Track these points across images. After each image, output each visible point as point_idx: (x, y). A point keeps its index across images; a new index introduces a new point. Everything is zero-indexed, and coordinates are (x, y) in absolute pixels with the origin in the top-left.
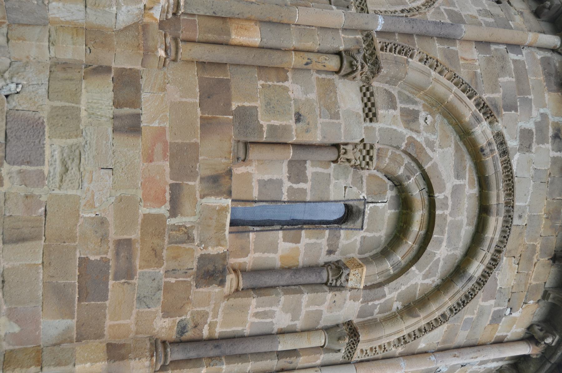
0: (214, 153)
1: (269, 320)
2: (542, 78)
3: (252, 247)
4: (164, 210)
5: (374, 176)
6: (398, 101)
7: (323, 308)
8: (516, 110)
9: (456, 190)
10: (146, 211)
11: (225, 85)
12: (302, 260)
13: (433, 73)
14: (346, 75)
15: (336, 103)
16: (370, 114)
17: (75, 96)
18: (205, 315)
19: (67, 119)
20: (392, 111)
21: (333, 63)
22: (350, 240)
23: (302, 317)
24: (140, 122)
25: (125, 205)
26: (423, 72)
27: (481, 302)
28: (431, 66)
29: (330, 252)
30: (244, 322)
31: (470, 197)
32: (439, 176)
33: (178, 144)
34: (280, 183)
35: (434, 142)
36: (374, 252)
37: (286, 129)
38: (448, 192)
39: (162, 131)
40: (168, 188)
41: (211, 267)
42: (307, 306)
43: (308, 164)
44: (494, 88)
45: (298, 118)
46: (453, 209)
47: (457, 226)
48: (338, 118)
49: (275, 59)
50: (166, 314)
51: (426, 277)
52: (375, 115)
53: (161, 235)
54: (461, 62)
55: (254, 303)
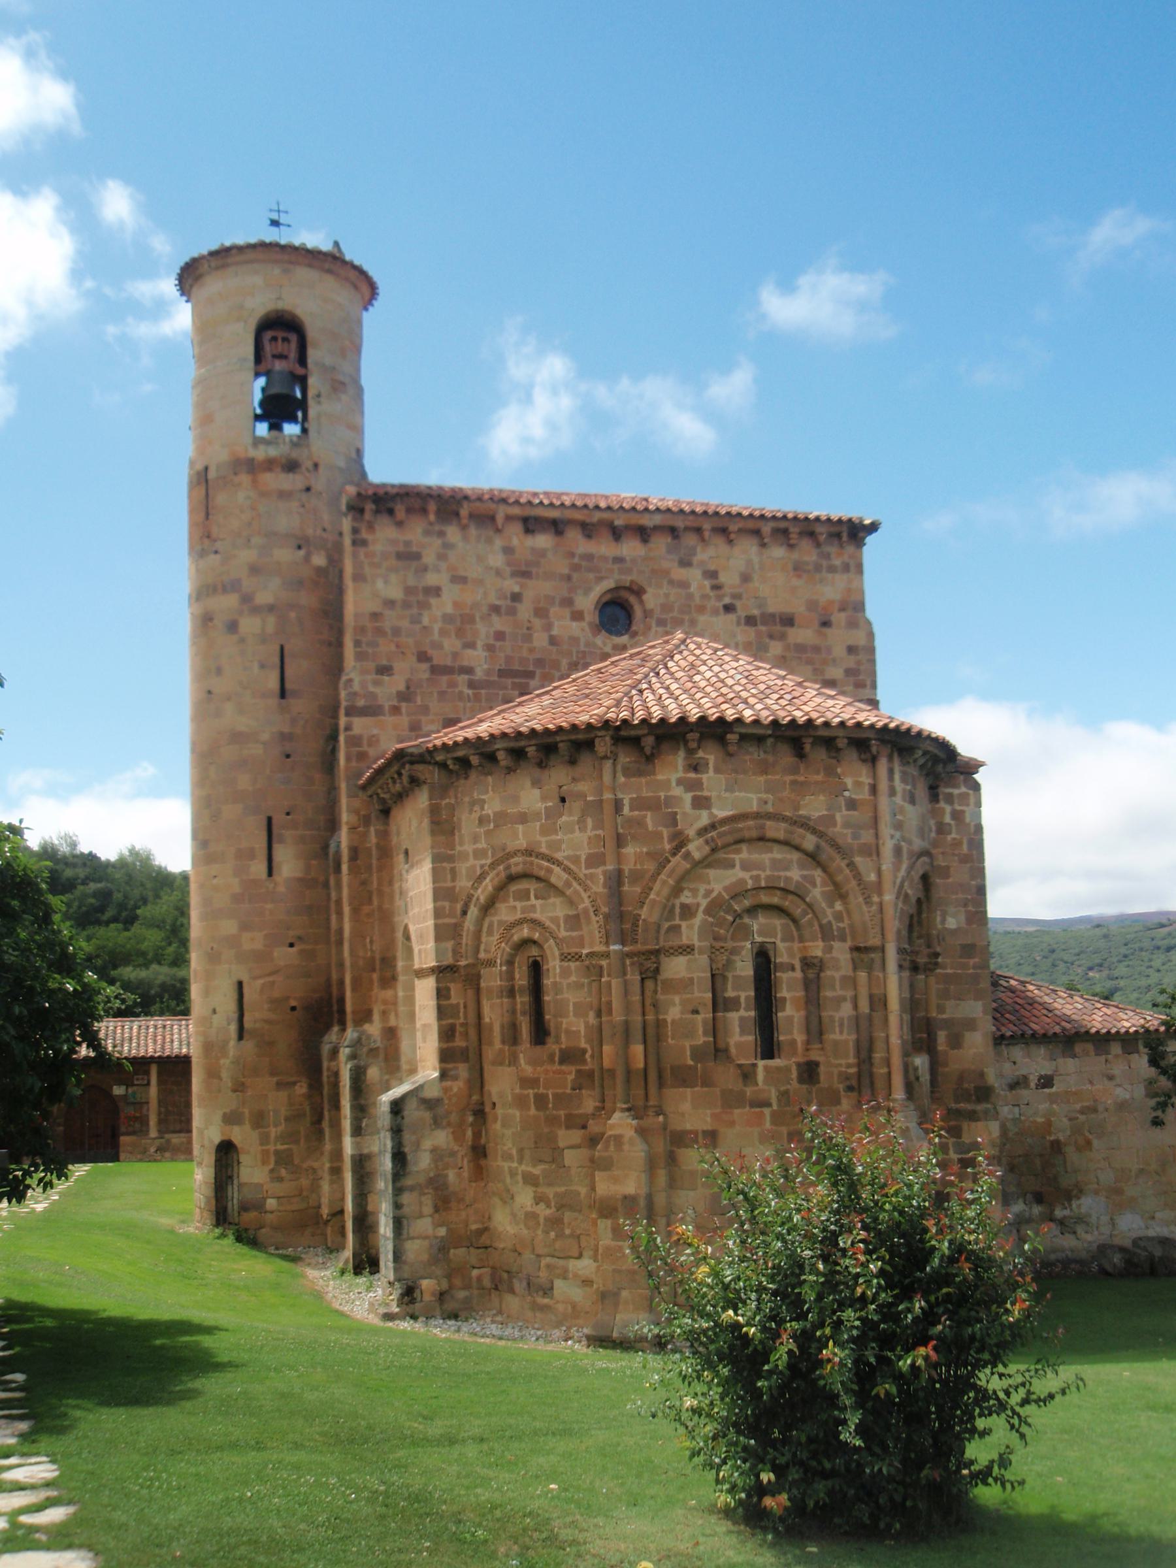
0: (727, 1078)
2: (643, 780)
3: (789, 1037)
4: (767, 1111)
5: (733, 934)
7: (837, 975)
8: (676, 813)
9: (745, 867)
11: (673, 1069)
13: (652, 896)
15: (681, 980)
16: (688, 950)
17: (693, 1173)
18: (840, 1073)
22: (785, 953)
25: (764, 1139)
27: (837, 829)
28: (646, 898)
29: (793, 969)
31: (749, 852)
34: (742, 1019)
36: (793, 928)
37: (705, 1022)
38: (746, 875)
39: (713, 1115)
41: (805, 1075)
42: (835, 990)
43: (727, 995)
44: (659, 836)
45: (696, 1012)
46: (760, 869)
47: (774, 862)
50: (838, 1102)
54: (639, 867)
55: (834, 1036)
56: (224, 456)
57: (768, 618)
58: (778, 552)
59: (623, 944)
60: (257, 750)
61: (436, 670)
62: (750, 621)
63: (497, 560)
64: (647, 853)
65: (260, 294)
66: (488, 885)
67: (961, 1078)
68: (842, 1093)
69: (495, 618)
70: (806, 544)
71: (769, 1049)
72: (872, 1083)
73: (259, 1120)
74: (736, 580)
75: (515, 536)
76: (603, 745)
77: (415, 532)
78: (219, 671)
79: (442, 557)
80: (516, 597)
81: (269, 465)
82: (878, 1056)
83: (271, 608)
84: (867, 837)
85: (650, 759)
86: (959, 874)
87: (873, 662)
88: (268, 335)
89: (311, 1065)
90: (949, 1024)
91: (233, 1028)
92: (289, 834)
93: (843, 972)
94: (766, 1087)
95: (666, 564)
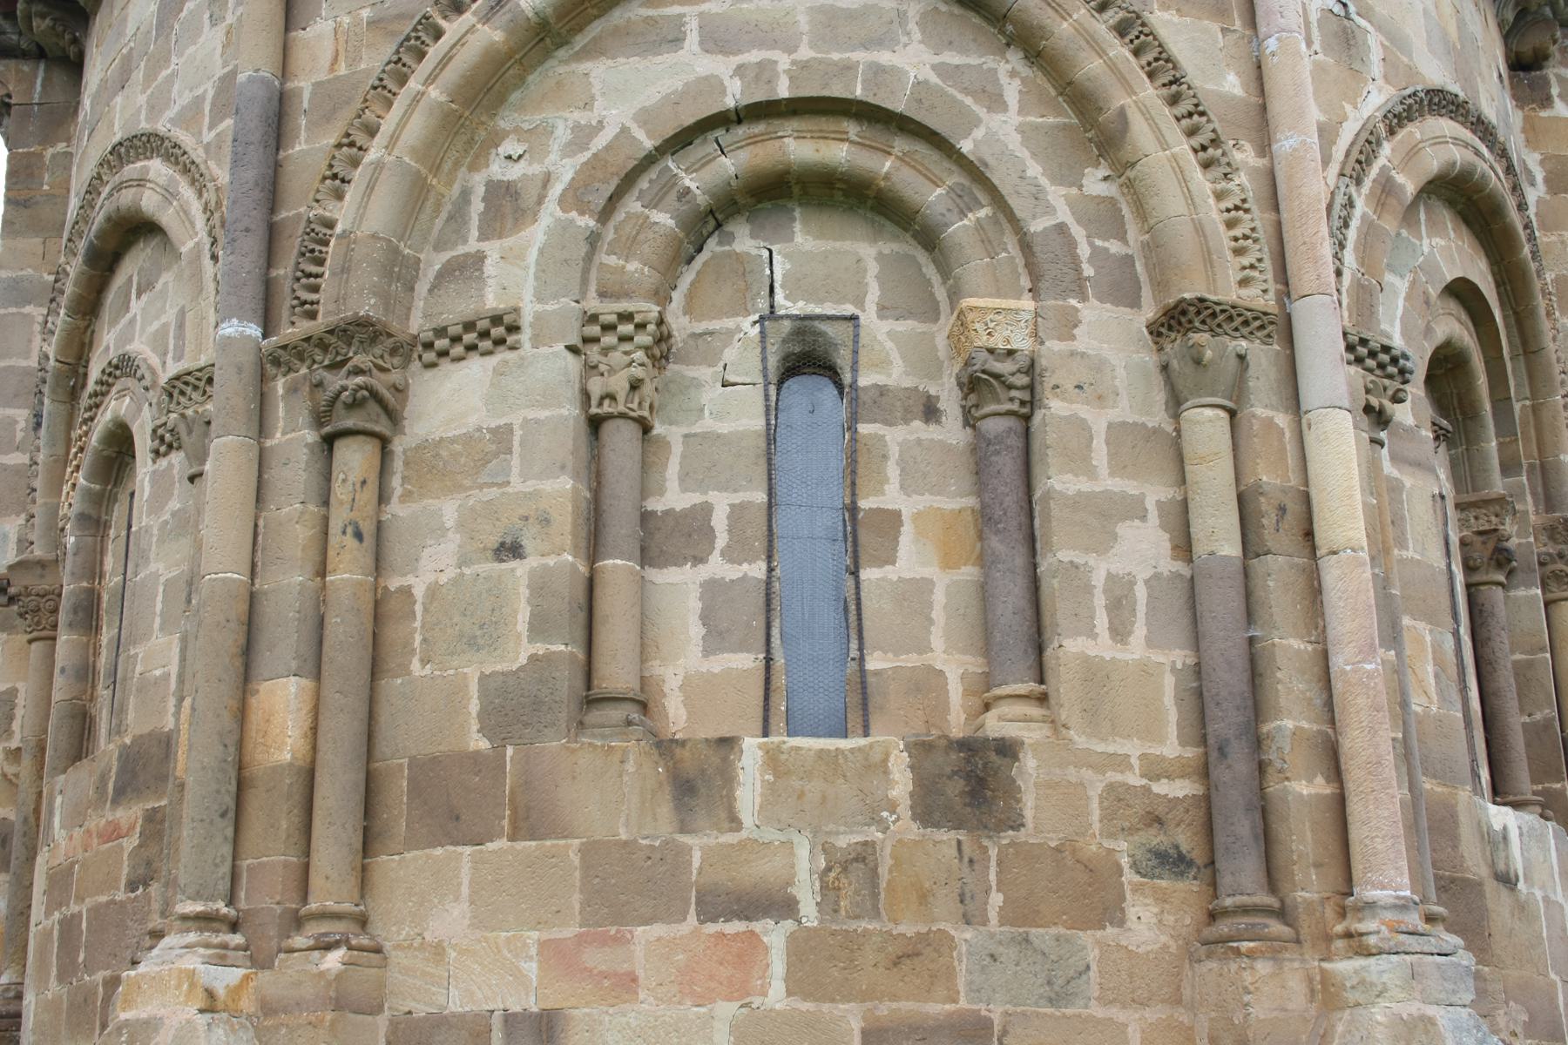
1: (1141, 592)
3: (911, 660)
4: (775, 935)
5: (690, 297)
6: (461, 250)
7: (1098, 420)
10: (777, 989)
11: (427, 771)
12: (957, 501)
13: (372, 155)
14: (393, 417)
15: (467, 439)
16: (495, 332)
18: (1116, 796)
20: (490, 268)
21: (354, 458)
23: (1131, 487)
24: (526, 1015)
26: (370, 187)
28: (355, 163)
29: (931, 412)
30: (1146, 670)
32: (675, 101)
33: (586, 904)
34: (712, 589)
35: (577, 128)
36: (930, 271)
37: (540, 586)
38: (720, 66)
40: (711, 928)
41: (955, 788)
42: (1091, 473)
43: (656, 505)
45: (510, 550)
46: (774, 44)
48: (509, 428)
49: (345, 629)
50: (1111, 913)
51: (996, 102)
52: (497, 320)
53: (851, 944)
54: (342, 70)
64: (372, 23)
68: (1129, 876)
72: (1267, 840)
82: (1291, 721)
93: (1122, 411)
94: (771, 835)
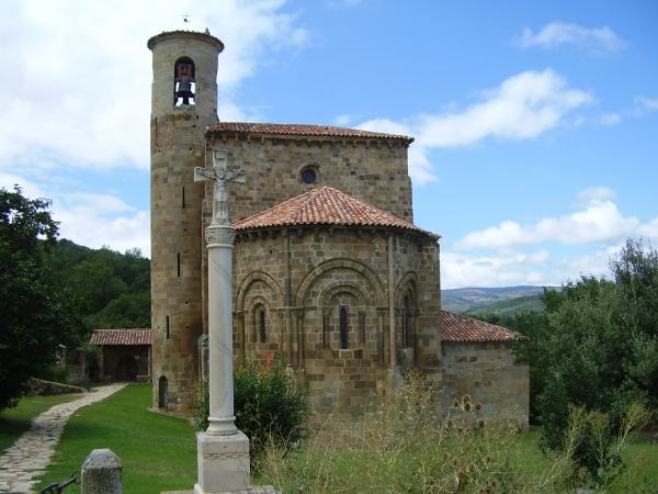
0: (327, 355)
9: (337, 278)
16: (315, 308)
19: (321, 392)
22: (351, 310)
25: (341, 378)
27: (372, 264)
44: (303, 266)
47: (349, 277)
49: (300, 338)
50: (369, 365)
56: (163, 114)
57: (368, 177)
58: (373, 150)
59: (290, 305)
60: (173, 228)
61: (238, 198)
62: (362, 178)
63: (262, 155)
65: (177, 51)
66: (246, 283)
67: (429, 356)
69: (261, 178)
70: (385, 148)
71: (344, 345)
73: (175, 369)
74: (356, 161)
75: (271, 148)
76: (284, 233)
77: (231, 145)
78: (160, 198)
79: (240, 155)
80: (269, 170)
81: (179, 117)
82: (386, 348)
83: (179, 173)
84: (384, 267)
85: (302, 237)
86: (430, 279)
87: (411, 193)
88: (180, 66)
89: (194, 350)
90: (424, 337)
91: (165, 334)
92: (186, 260)
95: (327, 156)
